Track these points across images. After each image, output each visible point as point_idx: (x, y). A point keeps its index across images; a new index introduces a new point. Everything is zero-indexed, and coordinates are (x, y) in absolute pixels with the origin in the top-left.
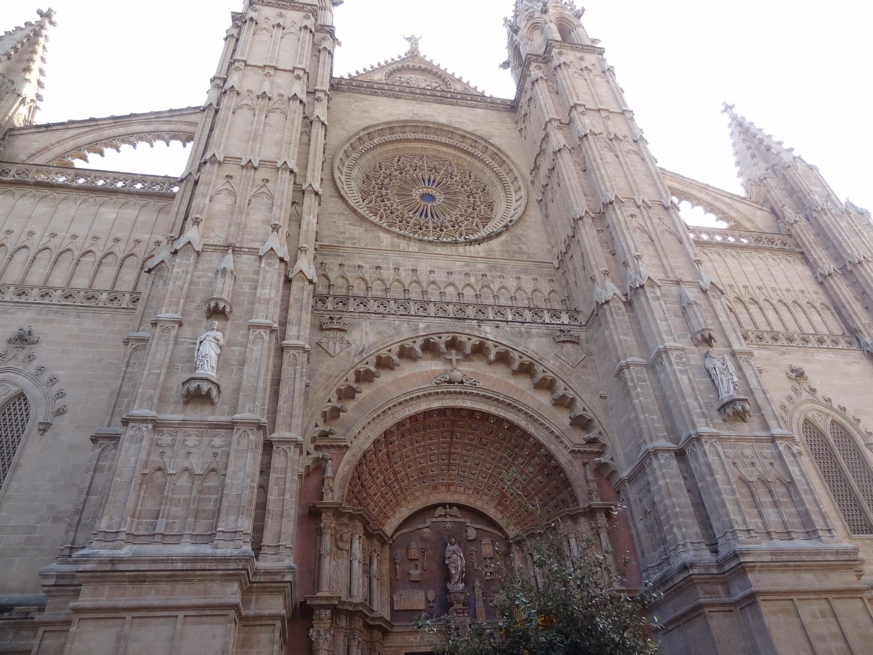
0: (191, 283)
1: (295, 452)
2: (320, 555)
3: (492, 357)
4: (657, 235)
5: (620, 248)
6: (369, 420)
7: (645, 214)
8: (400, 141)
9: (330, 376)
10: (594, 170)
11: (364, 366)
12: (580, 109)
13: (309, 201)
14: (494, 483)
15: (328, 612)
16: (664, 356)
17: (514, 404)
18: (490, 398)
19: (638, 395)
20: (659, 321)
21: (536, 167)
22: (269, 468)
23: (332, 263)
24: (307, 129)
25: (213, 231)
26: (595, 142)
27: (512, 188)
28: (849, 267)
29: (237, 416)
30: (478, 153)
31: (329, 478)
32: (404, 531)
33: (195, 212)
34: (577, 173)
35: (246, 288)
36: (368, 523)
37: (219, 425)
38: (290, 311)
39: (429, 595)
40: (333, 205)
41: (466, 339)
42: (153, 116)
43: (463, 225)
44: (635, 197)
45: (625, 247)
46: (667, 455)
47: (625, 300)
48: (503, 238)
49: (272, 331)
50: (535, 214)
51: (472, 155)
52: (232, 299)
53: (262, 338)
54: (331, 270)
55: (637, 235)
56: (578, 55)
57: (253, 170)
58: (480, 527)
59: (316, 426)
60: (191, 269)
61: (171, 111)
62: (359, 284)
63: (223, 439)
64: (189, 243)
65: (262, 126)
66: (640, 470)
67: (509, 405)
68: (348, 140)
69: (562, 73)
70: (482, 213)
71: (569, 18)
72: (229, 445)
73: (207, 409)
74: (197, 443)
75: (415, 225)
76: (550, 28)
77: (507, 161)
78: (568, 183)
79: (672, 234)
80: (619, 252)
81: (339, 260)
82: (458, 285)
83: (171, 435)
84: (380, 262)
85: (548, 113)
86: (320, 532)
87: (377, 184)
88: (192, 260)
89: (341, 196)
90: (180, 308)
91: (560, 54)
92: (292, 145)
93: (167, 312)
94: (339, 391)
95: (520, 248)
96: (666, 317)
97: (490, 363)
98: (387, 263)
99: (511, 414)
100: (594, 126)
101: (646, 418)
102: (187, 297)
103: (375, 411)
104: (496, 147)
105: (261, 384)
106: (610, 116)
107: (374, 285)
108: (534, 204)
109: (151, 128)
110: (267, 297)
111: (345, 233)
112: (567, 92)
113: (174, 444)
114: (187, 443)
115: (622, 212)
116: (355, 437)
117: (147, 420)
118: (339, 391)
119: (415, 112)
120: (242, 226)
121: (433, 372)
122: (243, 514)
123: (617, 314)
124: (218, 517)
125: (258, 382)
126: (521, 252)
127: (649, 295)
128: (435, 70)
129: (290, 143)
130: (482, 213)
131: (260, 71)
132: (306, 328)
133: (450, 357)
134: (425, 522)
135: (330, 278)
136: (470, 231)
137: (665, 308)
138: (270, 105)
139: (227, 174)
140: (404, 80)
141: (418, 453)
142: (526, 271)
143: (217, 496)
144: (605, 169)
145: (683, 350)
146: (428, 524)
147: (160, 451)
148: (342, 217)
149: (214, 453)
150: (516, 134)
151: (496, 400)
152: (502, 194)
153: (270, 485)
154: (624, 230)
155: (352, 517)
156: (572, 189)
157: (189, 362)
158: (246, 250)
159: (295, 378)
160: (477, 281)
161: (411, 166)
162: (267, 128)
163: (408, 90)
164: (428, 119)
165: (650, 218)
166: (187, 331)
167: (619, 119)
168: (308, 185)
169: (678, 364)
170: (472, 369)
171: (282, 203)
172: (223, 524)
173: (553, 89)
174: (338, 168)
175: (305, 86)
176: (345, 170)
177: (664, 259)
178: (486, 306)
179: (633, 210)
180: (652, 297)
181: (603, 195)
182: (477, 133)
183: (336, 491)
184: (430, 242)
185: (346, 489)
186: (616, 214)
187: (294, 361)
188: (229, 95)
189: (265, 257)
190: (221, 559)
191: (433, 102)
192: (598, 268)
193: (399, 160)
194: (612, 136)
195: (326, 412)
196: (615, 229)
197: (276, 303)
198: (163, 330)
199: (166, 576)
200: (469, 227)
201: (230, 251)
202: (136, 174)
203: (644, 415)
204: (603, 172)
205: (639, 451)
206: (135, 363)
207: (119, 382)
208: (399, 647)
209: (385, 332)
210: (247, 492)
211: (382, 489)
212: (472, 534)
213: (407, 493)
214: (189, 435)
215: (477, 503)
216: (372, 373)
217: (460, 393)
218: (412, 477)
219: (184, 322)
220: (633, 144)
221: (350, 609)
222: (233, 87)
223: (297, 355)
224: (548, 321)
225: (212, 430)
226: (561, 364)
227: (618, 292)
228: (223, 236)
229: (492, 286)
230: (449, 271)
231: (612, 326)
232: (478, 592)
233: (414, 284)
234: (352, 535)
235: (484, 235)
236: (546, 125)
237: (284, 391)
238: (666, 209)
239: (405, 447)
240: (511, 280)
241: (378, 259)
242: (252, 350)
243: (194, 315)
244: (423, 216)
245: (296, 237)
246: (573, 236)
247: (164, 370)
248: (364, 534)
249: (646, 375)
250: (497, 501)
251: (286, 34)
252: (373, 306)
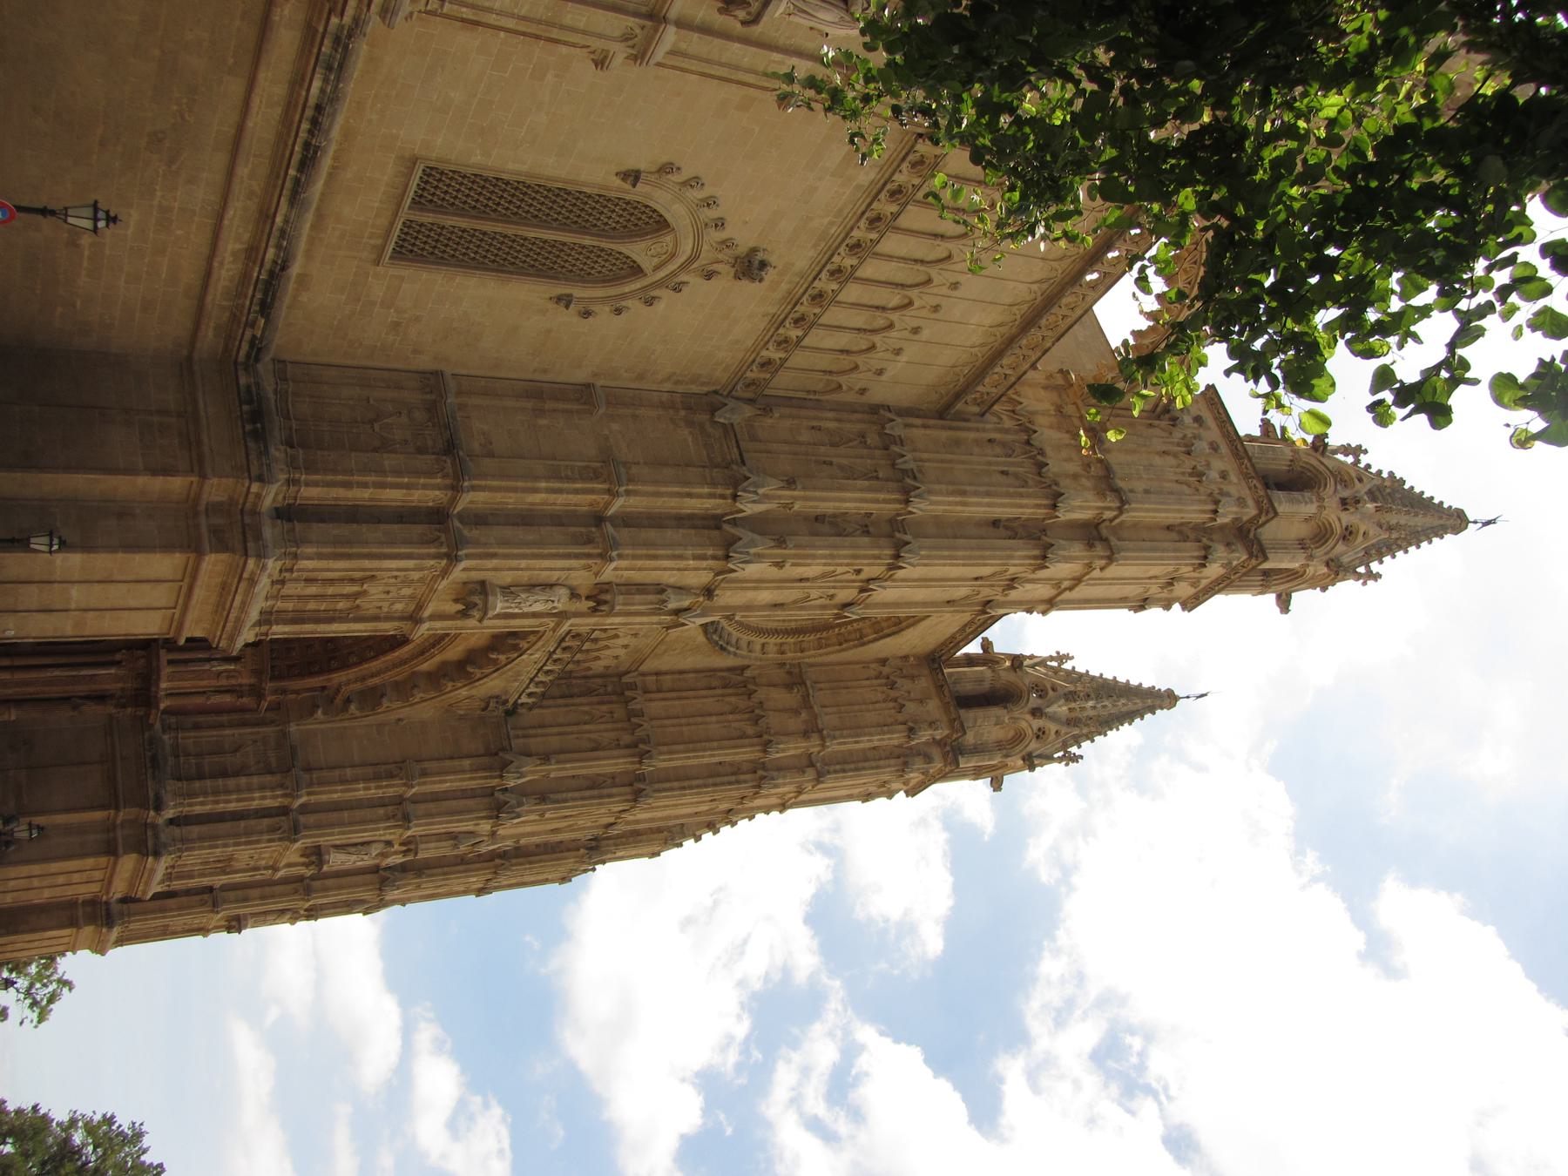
28: (498, 861)
67: (423, 653)
77: (838, 647)
104: (870, 642)
150: (882, 655)
181: (659, 791)
199: (225, 603)
236: (823, 739)
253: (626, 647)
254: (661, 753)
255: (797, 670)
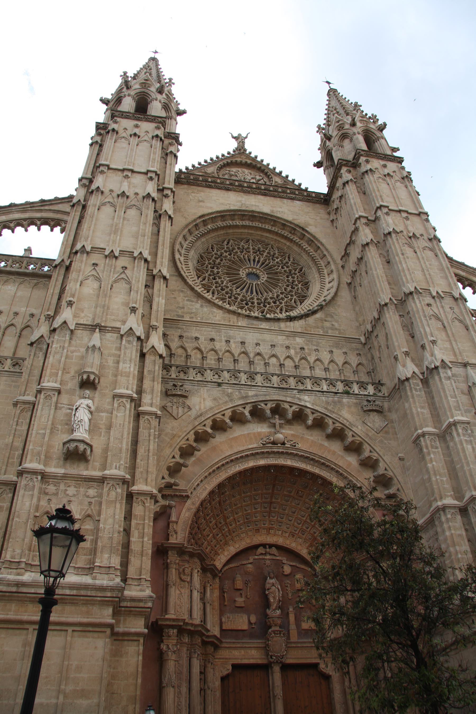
0: (67, 357)
1: (150, 502)
2: (167, 585)
3: (310, 422)
4: (448, 322)
5: (418, 333)
6: (206, 474)
7: (439, 304)
8: (230, 227)
9: (174, 436)
10: (396, 263)
11: (202, 428)
12: (385, 210)
13: (159, 285)
14: (307, 528)
15: (175, 631)
16: (453, 428)
17: (327, 463)
18: (307, 458)
19: (431, 461)
20: (449, 398)
21: (346, 255)
22: (131, 515)
23: (173, 335)
24: (156, 222)
25: (83, 312)
26: (397, 240)
27: (325, 271)
29: (107, 472)
30: (296, 239)
31: (173, 522)
32: (231, 566)
33: (69, 295)
34: (383, 265)
35: (111, 362)
36: (204, 560)
37: (92, 479)
38: (145, 381)
39: (251, 618)
40: (175, 283)
41: (288, 407)
42: (29, 206)
43: (283, 302)
44: (430, 288)
45: (423, 332)
46: (452, 511)
47: (422, 377)
48: (318, 315)
49: (132, 399)
50: (345, 294)
51: (291, 241)
52: (99, 372)
53: (125, 406)
54: (173, 340)
55: (433, 322)
56: (382, 162)
57: (114, 259)
58: (294, 564)
59: (163, 478)
60: (66, 345)
61: (43, 201)
62: (196, 353)
63: (96, 490)
64: (65, 322)
65: (122, 220)
66: (431, 522)
67: (323, 464)
68: (187, 226)
69: (368, 178)
70: (299, 292)
71: (373, 131)
72: (100, 496)
73: (82, 466)
74: (75, 493)
75: (242, 300)
76: (357, 139)
77: (321, 247)
78: (374, 272)
79: (460, 321)
80: (417, 335)
81: (179, 332)
82: (280, 356)
83: (55, 486)
84: (213, 334)
85: (357, 210)
86: (167, 567)
87: (210, 264)
88: (68, 338)
89: (180, 276)
90: (59, 378)
91: (367, 162)
92: (146, 237)
93: (49, 381)
94: (181, 449)
95: (332, 325)
96: (455, 395)
97: (308, 428)
98: (219, 335)
99: (324, 472)
100: (396, 225)
101: (437, 479)
102: (64, 369)
103: (211, 467)
105: (124, 446)
106: (410, 216)
107: (209, 355)
108: (344, 286)
109: (27, 215)
110: (128, 370)
111: (183, 308)
112: (373, 194)
113: (58, 493)
114: (68, 492)
115: (420, 301)
116: (195, 489)
117: (37, 472)
118: (181, 449)
119: (243, 202)
120: (106, 308)
121: (259, 434)
122: (114, 553)
123: (416, 390)
124: (95, 554)
125: (121, 443)
126: (333, 328)
127: (441, 374)
128: (259, 166)
129: (144, 236)
130: (299, 292)
131: (120, 173)
132: (157, 396)
133: (274, 421)
134: (249, 559)
135: (172, 347)
136: (290, 308)
137: (455, 387)
138: (128, 203)
139: (93, 262)
140: (233, 173)
141: (244, 502)
142: (337, 346)
143: (92, 537)
144: (406, 263)
145: (468, 423)
146: (251, 560)
147: (48, 498)
148: (182, 294)
149: (89, 502)
150: (329, 224)
151: (312, 459)
152: (317, 275)
153: (132, 529)
154: (422, 317)
155: (192, 555)
156: (378, 278)
157: (67, 424)
158: (110, 329)
159: (149, 440)
160: (296, 353)
161: (239, 248)
162: (125, 222)
163: (237, 184)
164: (254, 209)
165: (442, 307)
166: (64, 398)
167: (415, 219)
168: (158, 270)
169: (464, 435)
170: (292, 432)
171: (138, 288)
172: (99, 561)
173: (361, 189)
174: (178, 251)
175: (156, 186)
176: (183, 252)
177: (454, 343)
178: (305, 378)
179: (428, 300)
180: (445, 377)
181: (404, 286)
182: (296, 222)
183: (179, 534)
184: (256, 318)
185: (187, 532)
186: (415, 303)
187: (148, 425)
188: (95, 195)
189: (125, 336)
190: (99, 588)
191: (258, 194)
192: (400, 349)
193: (228, 243)
194: (411, 235)
195: (171, 466)
196: (414, 316)
197: (134, 375)
198: (46, 397)
200: (288, 304)
201: (97, 330)
202: (15, 256)
203: (436, 477)
204: (404, 266)
205: (430, 506)
206: (22, 422)
207: (11, 438)
208: (226, 659)
209: (220, 398)
210: (116, 535)
211: (214, 531)
212: (287, 570)
213: (234, 534)
214: (69, 486)
215: (293, 545)
216: (209, 434)
217: (282, 453)
218: (239, 521)
219: (62, 390)
220: (428, 241)
221: (192, 628)
222: (98, 187)
223: (150, 419)
224: (356, 392)
225: (87, 483)
226: (367, 430)
227: (417, 371)
228: (91, 315)
229: (308, 358)
230: (273, 343)
231: (411, 400)
232: (292, 618)
233: (242, 355)
234: (192, 569)
235: (302, 312)
237: (141, 451)
238: (456, 299)
239: (234, 496)
240: (325, 353)
241: (212, 331)
242: (117, 416)
243: (69, 384)
244: (249, 293)
245: (148, 316)
246: (379, 319)
247: (48, 431)
248: (201, 569)
249: (438, 443)
250: (309, 543)
251: (141, 142)
252: (209, 375)
253: (331, 352)
254: (380, 298)
255: (344, 259)
